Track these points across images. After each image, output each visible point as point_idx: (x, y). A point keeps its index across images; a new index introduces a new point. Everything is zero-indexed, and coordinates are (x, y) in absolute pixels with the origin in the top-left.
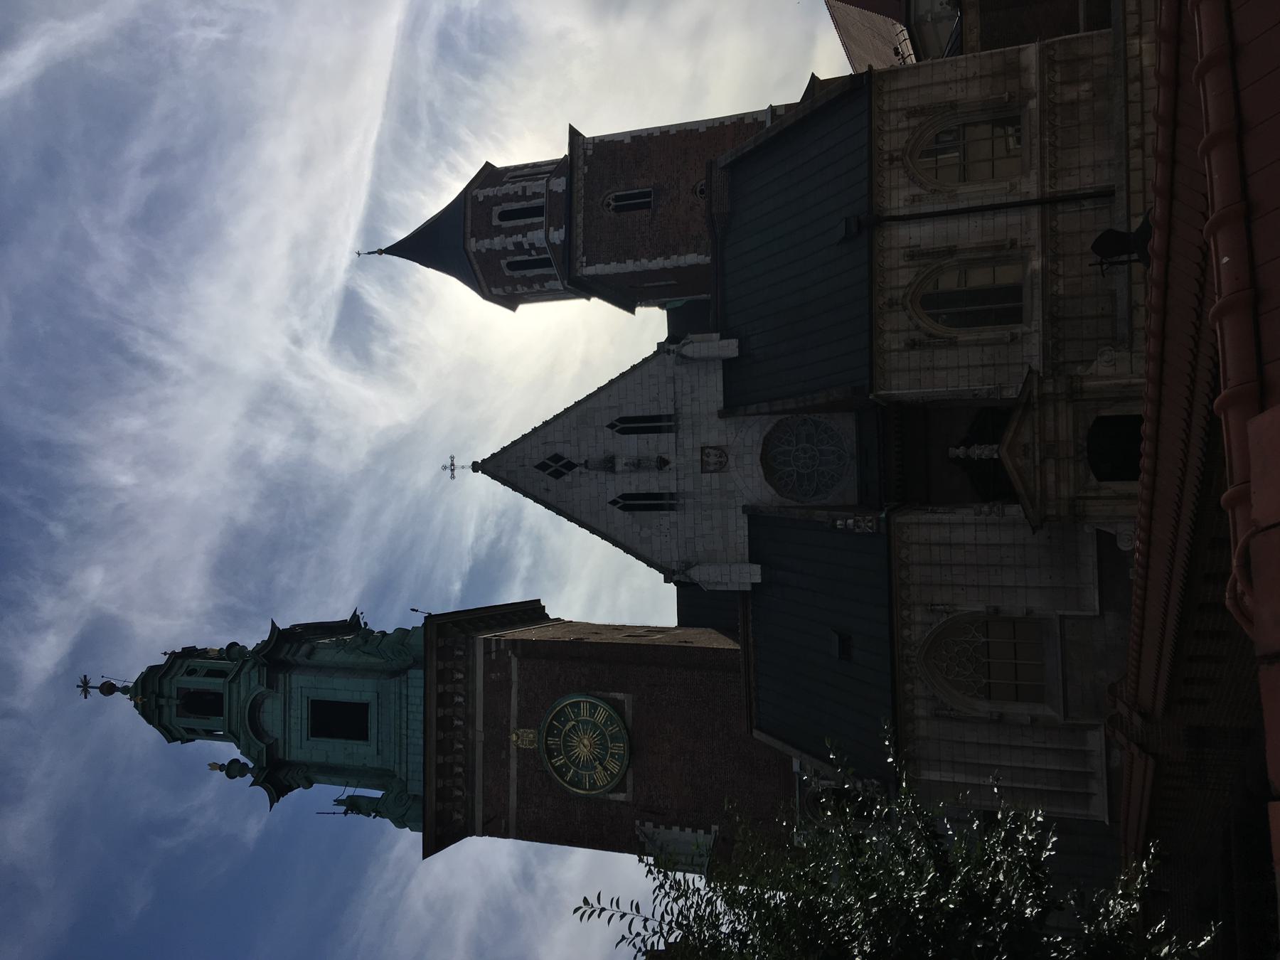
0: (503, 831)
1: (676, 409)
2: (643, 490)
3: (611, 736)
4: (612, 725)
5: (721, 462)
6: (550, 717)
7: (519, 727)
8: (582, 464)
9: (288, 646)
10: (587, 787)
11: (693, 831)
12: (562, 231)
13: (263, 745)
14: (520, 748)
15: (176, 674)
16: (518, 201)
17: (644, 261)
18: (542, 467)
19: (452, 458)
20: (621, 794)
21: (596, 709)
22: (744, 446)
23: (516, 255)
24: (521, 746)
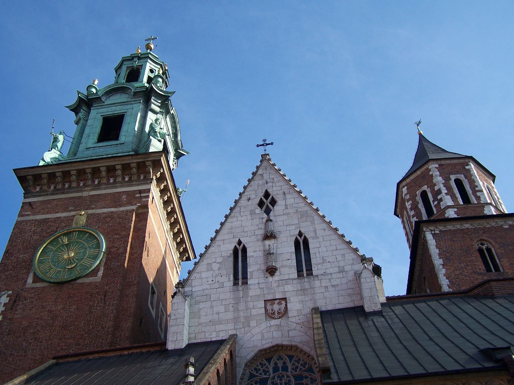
0: (23, 213)
1: (317, 276)
2: (250, 261)
5: (274, 314)
6: (91, 232)
8: (269, 218)
9: (160, 101)
12: (456, 216)
13: (101, 95)
15: (150, 64)
16: (471, 188)
17: (444, 271)
18: (267, 195)
19: (272, 144)
20: (32, 280)
22: (289, 331)
23: (431, 193)
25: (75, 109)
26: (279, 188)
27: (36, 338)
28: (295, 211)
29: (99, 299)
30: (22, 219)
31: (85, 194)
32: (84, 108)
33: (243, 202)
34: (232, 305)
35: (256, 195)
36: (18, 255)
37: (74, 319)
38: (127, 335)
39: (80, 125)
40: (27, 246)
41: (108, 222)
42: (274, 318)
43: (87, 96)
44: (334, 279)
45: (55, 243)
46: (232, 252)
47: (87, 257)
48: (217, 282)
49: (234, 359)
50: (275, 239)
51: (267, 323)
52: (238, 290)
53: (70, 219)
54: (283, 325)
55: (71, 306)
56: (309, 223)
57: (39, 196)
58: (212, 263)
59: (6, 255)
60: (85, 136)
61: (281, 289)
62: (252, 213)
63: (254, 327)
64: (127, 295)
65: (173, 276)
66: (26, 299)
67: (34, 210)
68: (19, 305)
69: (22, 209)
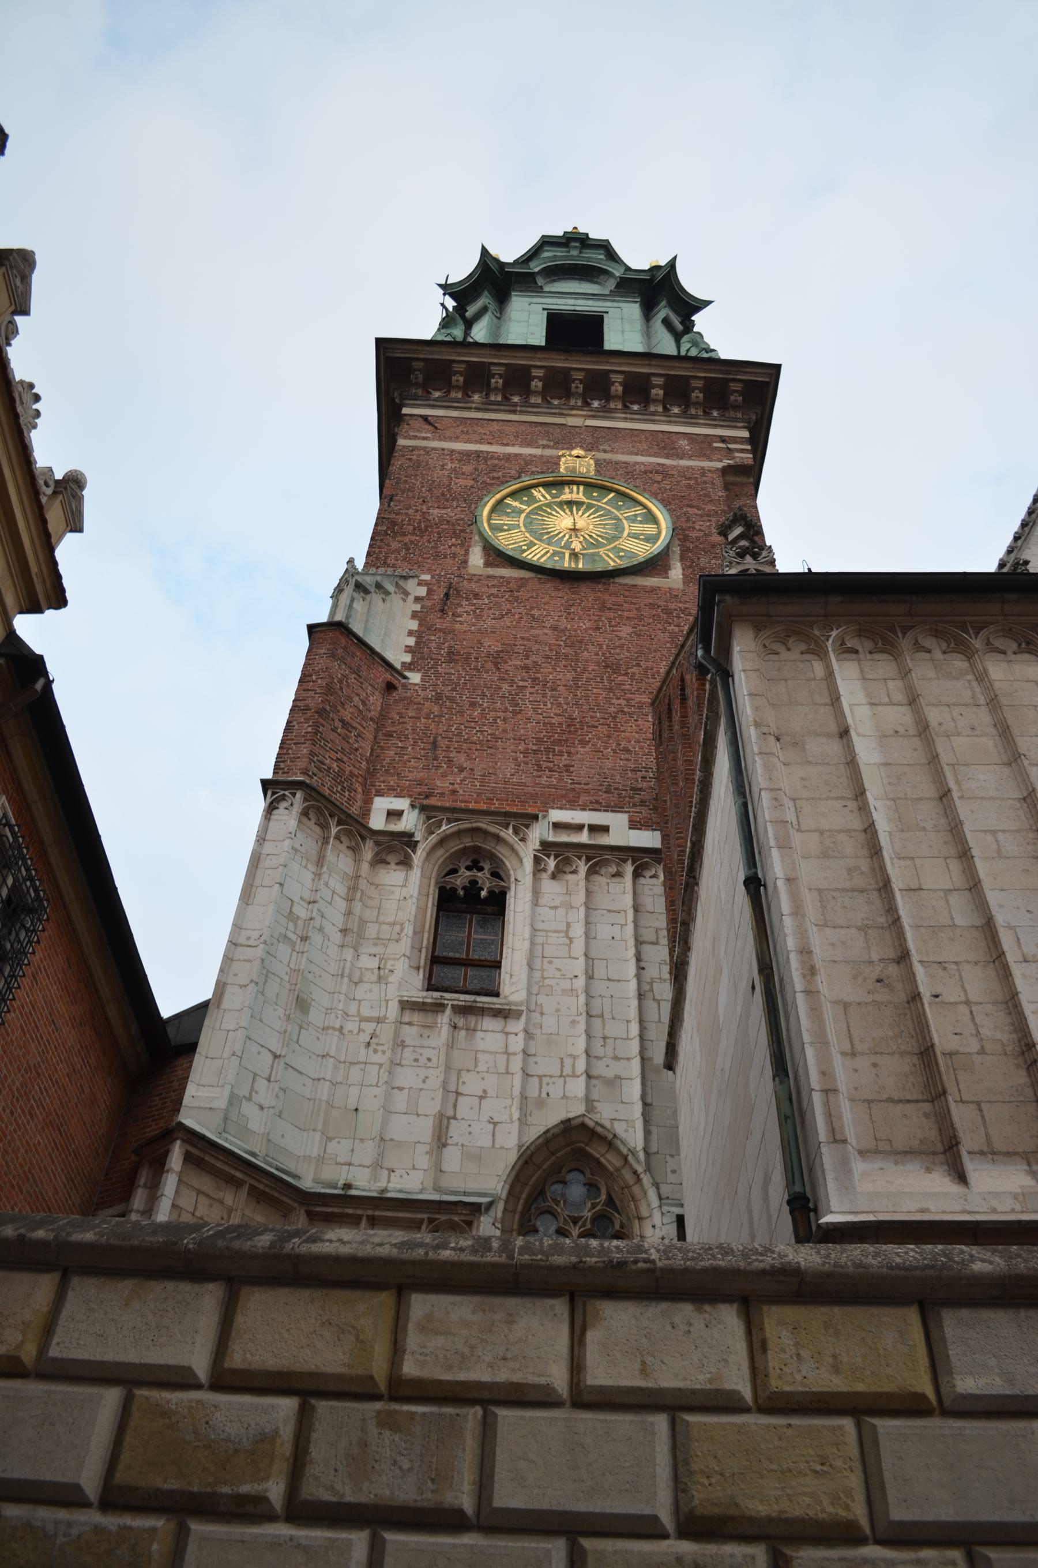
0: (412, 434)
7: (598, 463)
24: (563, 459)
27: (534, 679)
31: (571, 421)
40: (443, 494)
41: (658, 482)
45: (525, 499)
55: (616, 626)
66: (477, 596)
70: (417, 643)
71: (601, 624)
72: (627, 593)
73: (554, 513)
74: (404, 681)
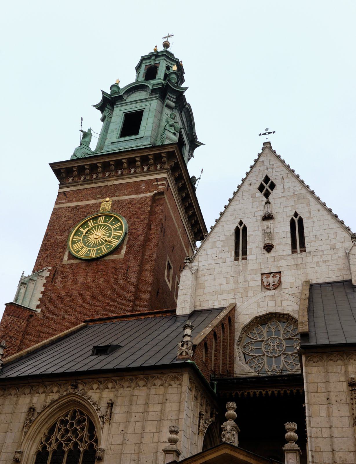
0: (59, 201)
1: (309, 252)
2: (249, 239)
3: (100, 249)
4: (107, 248)
5: (269, 285)
6: (115, 216)
8: (268, 201)
9: (175, 97)
10: (74, 240)
11: (40, 298)
13: (122, 94)
14: (101, 204)
20: (67, 258)
21: (118, 239)
24: (102, 204)
25: (101, 107)
26: (278, 173)
28: (292, 194)
29: (122, 273)
30: (58, 206)
31: (110, 183)
32: (108, 106)
33: (245, 187)
34: (232, 278)
35: (257, 181)
36: (56, 237)
37: (102, 290)
38: (145, 303)
39: (105, 121)
40: (63, 229)
41: (130, 208)
42: (269, 289)
43: (111, 95)
44: (325, 256)
45: (85, 227)
46: (234, 231)
47: (112, 238)
48: (220, 258)
49: (232, 324)
50: (272, 219)
51: (262, 293)
52: (238, 265)
53: (98, 206)
54: (277, 295)
55: (99, 279)
56: (305, 205)
57: (72, 186)
58: (216, 242)
59: (46, 237)
60: (109, 132)
61: (276, 264)
62: (253, 196)
63: (251, 297)
64: (146, 270)
65: (188, 253)
66: (63, 274)
67: (68, 198)
68: (57, 278)
69: (58, 198)
70: (43, 296)
71: (95, 279)
72: (106, 264)
73: (89, 235)
74: (36, 312)
